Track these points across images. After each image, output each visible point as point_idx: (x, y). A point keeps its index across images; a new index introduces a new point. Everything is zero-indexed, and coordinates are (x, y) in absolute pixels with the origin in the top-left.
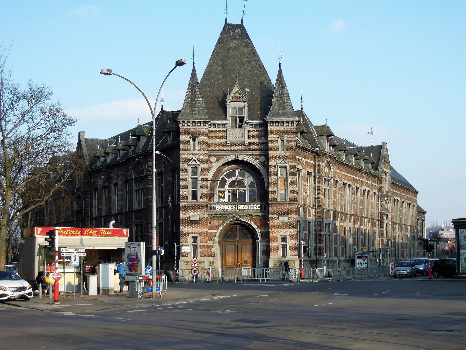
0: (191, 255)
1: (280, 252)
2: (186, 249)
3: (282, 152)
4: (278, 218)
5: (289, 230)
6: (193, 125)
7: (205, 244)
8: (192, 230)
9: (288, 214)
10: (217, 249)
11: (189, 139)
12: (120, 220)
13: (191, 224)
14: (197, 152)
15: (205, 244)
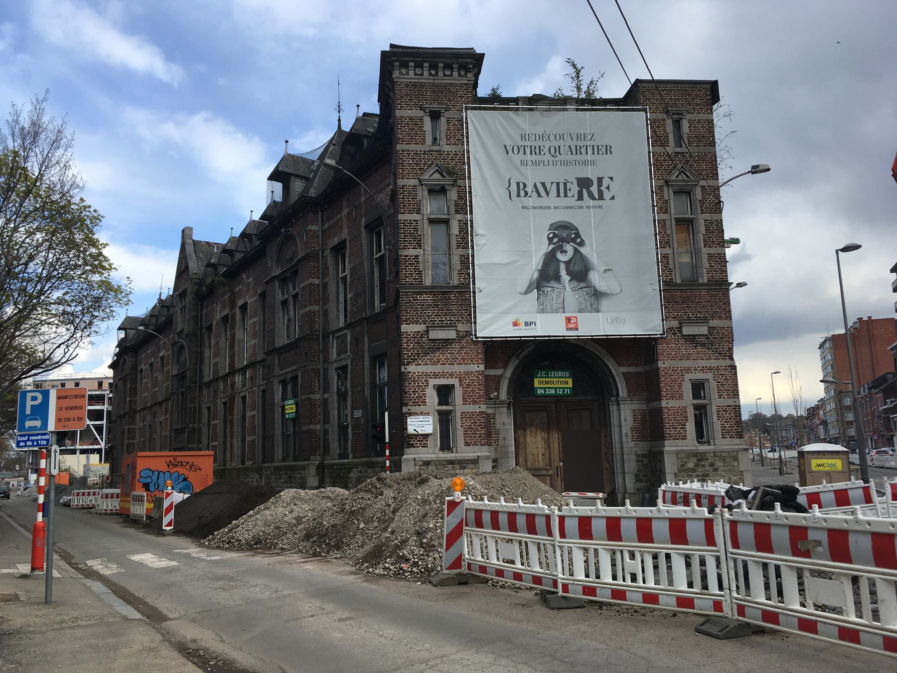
0: (435, 440)
1: (691, 427)
2: (421, 424)
3: (679, 150)
4: (680, 329)
5: (714, 363)
6: (430, 74)
7: (476, 408)
8: (437, 369)
9: (704, 320)
10: (505, 421)
11: (421, 113)
12: (252, 378)
13: (434, 350)
14: (446, 148)
15: (476, 408)
